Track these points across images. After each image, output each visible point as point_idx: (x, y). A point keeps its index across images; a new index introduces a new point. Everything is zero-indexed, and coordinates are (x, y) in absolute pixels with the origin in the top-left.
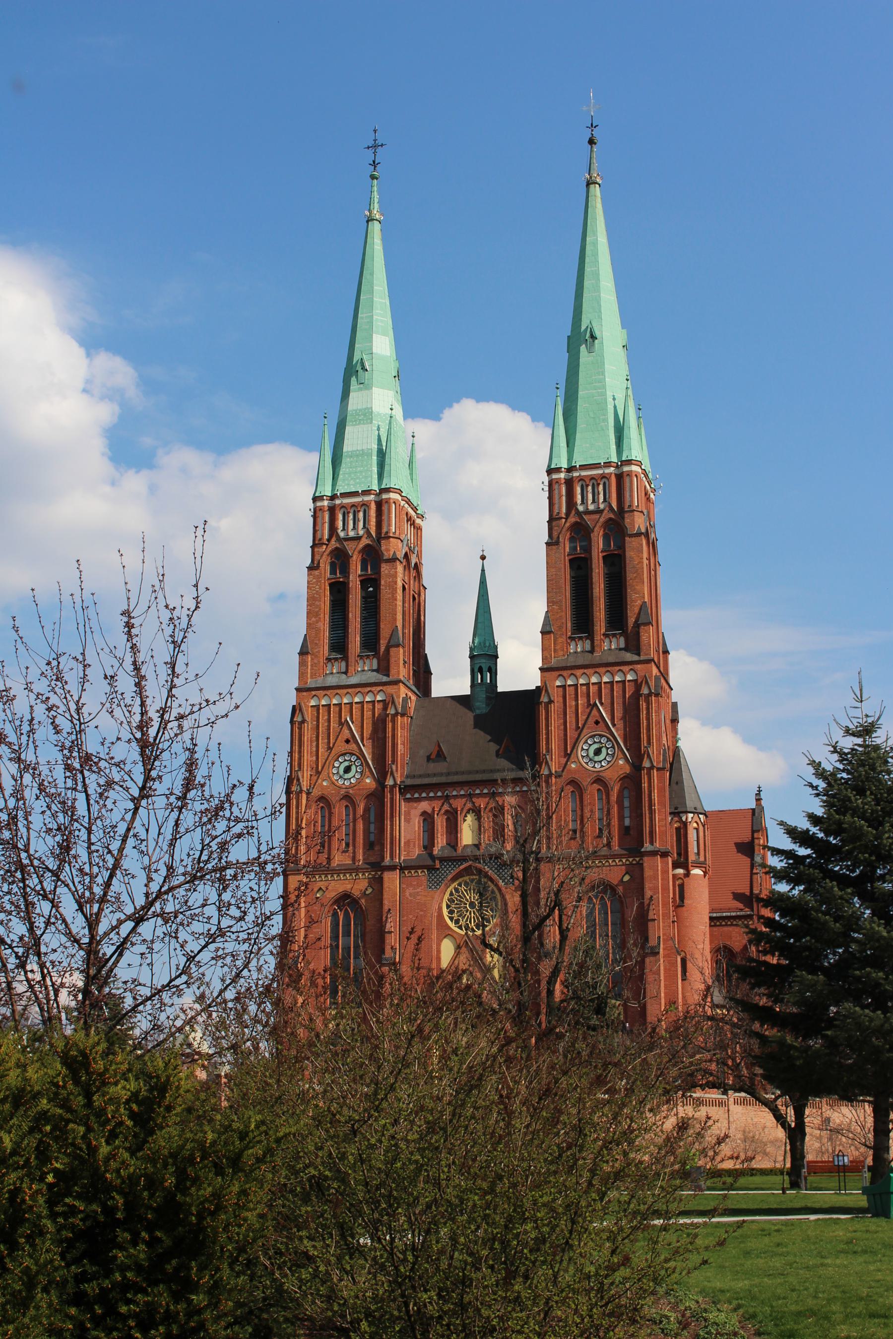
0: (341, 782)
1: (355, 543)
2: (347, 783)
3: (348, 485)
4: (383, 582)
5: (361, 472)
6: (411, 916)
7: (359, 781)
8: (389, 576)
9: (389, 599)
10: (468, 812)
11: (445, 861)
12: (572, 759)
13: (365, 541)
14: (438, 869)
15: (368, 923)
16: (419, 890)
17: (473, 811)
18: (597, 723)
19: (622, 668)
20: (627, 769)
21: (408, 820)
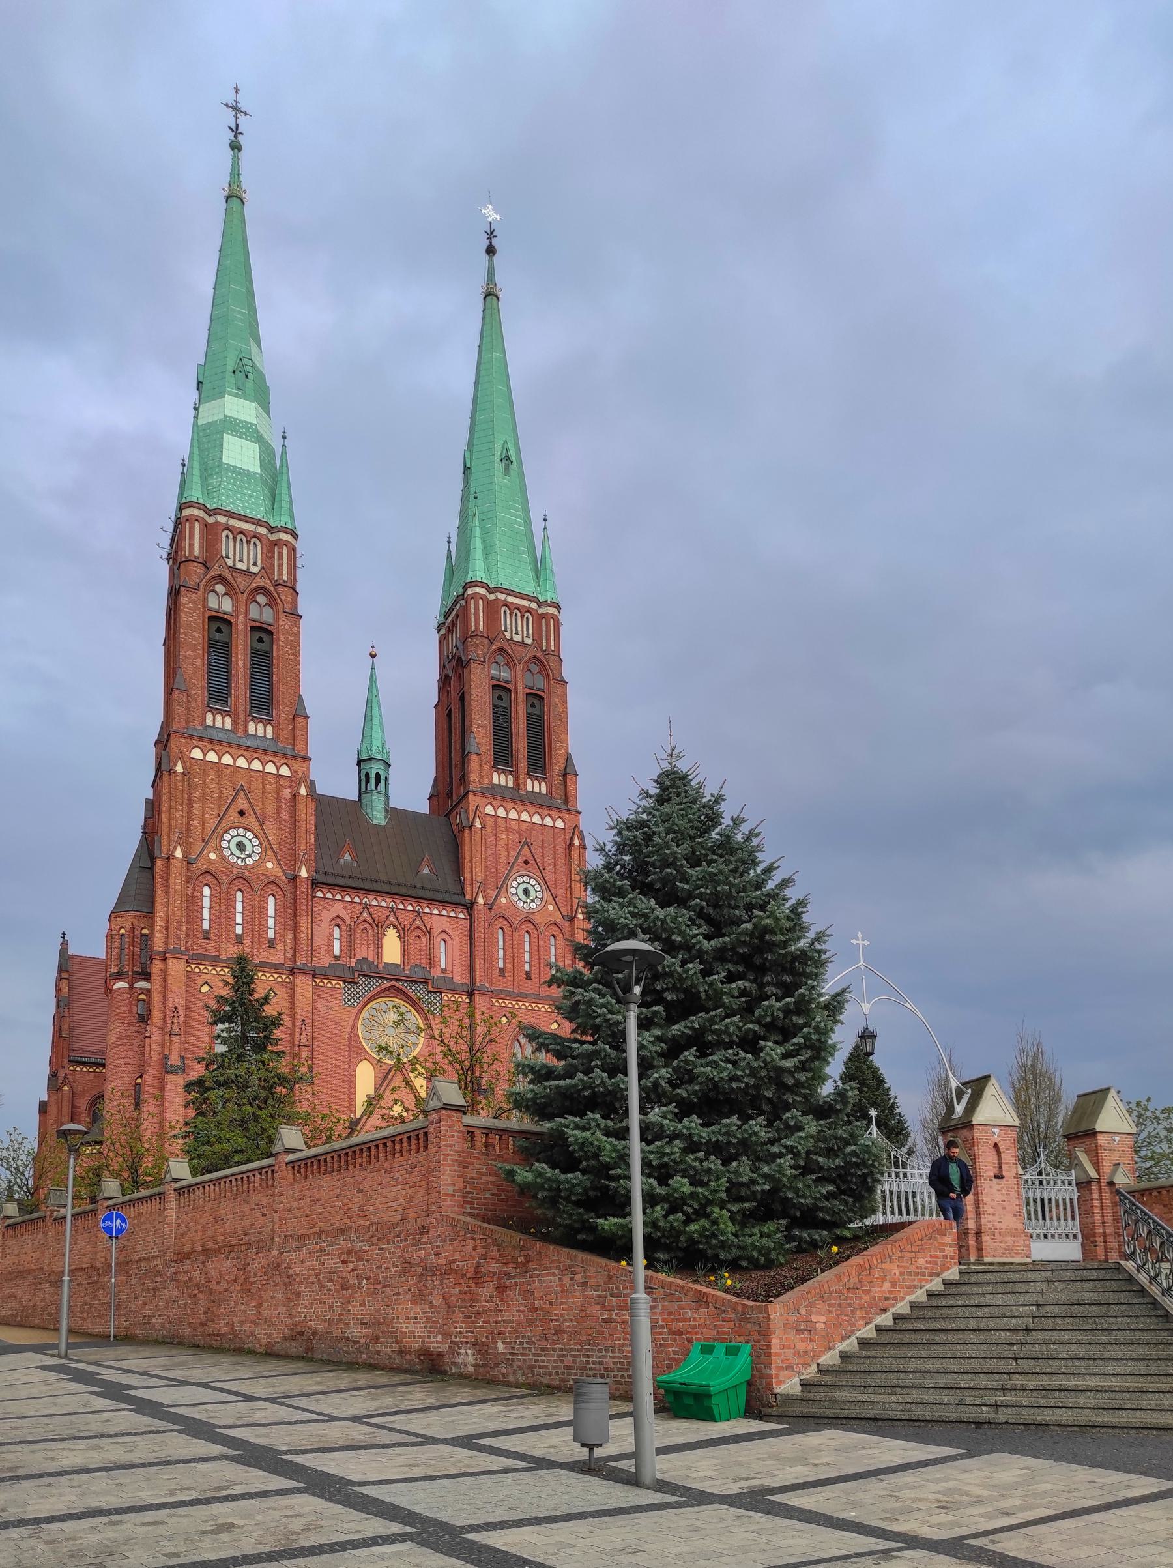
0: (233, 859)
1: (248, 579)
4: (282, 638)
10: (388, 927)
11: (364, 976)
13: (259, 582)
14: (356, 983)
16: (333, 1003)
17: (395, 927)
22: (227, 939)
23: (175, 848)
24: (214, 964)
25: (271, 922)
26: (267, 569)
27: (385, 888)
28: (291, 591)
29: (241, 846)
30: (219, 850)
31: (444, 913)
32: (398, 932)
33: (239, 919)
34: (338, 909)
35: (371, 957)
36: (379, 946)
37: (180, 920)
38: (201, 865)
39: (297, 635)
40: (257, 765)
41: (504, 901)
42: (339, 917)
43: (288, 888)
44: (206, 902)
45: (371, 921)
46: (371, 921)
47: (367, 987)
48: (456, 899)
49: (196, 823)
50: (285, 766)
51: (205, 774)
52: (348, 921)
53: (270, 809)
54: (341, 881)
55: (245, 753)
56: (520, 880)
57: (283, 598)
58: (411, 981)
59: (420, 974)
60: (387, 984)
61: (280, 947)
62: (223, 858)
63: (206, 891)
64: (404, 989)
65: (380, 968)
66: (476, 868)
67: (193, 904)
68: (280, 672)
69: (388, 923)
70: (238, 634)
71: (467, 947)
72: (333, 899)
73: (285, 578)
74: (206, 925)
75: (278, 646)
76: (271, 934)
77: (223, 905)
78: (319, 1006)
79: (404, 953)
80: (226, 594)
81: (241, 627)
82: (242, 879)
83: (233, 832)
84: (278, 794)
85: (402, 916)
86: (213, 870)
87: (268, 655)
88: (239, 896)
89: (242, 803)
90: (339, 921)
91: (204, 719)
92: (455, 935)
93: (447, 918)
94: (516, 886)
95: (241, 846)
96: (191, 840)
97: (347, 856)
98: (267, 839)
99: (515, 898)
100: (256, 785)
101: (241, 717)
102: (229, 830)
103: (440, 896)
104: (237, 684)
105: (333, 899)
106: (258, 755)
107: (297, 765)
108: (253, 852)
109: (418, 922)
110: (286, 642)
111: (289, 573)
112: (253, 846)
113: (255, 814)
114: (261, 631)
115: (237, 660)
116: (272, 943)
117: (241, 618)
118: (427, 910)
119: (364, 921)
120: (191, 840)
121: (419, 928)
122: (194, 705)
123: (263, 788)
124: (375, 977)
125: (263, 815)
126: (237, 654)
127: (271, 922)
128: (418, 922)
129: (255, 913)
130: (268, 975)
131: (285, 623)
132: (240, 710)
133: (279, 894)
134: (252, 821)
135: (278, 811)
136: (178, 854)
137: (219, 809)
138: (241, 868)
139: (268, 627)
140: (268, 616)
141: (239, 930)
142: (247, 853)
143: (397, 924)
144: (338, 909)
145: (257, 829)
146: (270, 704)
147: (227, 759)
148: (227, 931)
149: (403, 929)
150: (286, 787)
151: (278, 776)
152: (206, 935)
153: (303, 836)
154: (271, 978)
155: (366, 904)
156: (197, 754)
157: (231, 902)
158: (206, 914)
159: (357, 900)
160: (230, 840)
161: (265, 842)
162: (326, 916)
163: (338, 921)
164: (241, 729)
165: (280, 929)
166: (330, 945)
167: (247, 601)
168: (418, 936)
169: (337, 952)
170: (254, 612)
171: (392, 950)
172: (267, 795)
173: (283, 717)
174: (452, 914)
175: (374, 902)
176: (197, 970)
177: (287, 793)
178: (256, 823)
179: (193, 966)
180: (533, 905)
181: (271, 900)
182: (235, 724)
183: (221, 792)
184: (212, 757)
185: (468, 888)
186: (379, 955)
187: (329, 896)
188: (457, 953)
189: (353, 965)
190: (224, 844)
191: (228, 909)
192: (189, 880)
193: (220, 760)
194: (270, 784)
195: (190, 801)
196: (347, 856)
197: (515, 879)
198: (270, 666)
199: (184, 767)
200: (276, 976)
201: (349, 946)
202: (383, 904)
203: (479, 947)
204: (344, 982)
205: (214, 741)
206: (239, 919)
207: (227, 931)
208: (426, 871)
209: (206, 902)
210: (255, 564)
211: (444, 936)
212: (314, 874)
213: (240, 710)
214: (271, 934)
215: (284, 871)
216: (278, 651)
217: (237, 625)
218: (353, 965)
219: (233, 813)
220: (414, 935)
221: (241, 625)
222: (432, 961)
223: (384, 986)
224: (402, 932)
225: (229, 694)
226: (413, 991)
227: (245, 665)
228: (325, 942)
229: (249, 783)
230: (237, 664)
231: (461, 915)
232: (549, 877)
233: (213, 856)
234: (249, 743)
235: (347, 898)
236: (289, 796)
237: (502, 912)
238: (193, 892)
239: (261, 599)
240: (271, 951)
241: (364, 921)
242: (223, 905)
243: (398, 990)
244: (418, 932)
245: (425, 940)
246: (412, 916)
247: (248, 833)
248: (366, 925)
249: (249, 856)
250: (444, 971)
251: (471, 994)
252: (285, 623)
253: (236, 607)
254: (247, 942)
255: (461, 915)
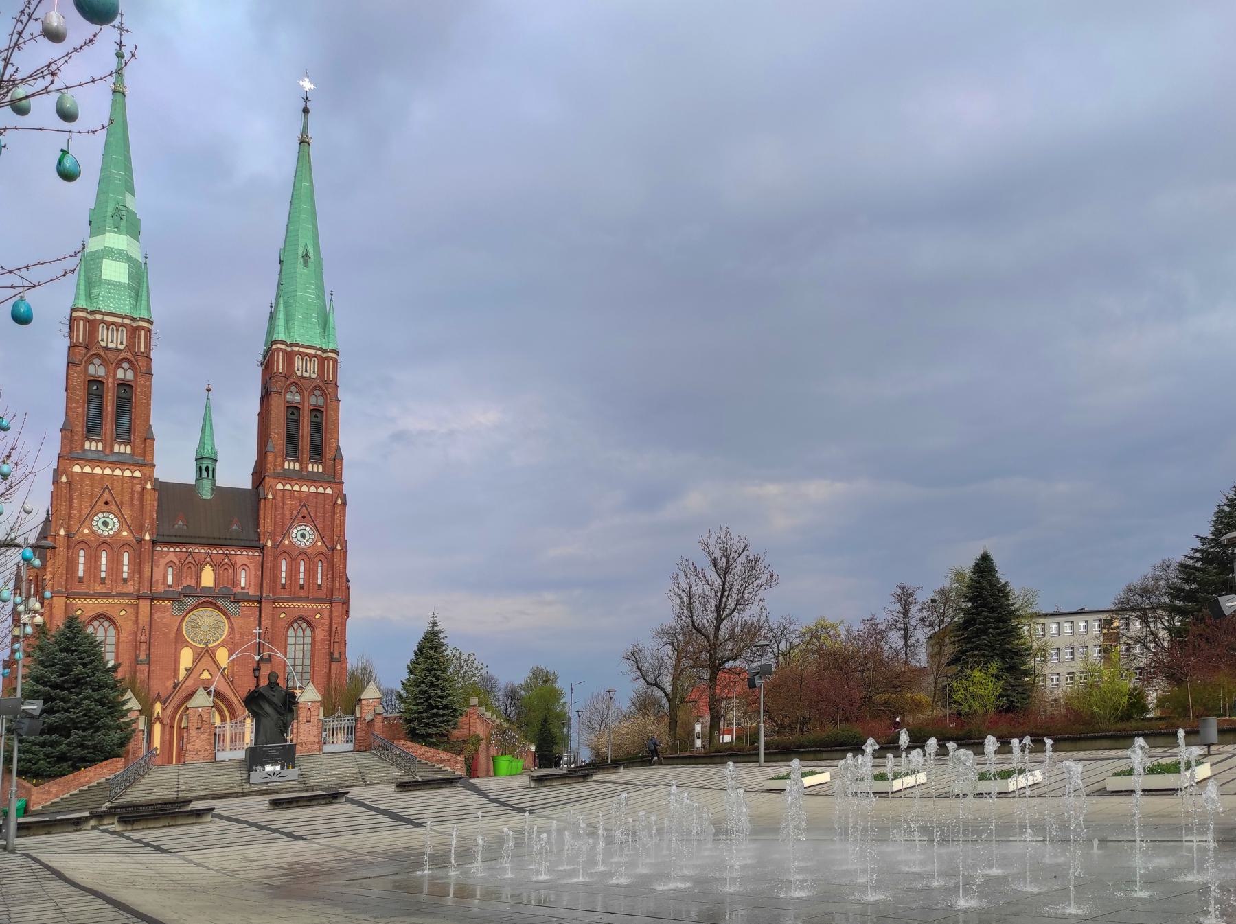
0: (100, 532)
2: (105, 534)
3: (108, 306)
4: (139, 390)
5: (120, 300)
6: (158, 632)
7: (117, 534)
8: (144, 386)
9: (145, 403)
10: (206, 564)
12: (285, 538)
13: (124, 355)
15: (121, 636)
17: (210, 564)
18: (304, 517)
19: (323, 485)
20: (324, 550)
21: (158, 567)
22: (95, 582)
23: (60, 529)
24: (85, 597)
25: (125, 568)
26: (131, 345)
27: (204, 541)
28: (146, 358)
29: (105, 524)
30: (90, 527)
31: (245, 553)
32: (212, 567)
33: (103, 568)
34: (171, 557)
35: (193, 584)
36: (198, 577)
37: (62, 573)
38: (78, 538)
39: (150, 386)
40: (118, 472)
41: (287, 542)
42: (172, 561)
43: (136, 547)
44: (81, 560)
45: (194, 562)
46: (194, 562)
47: (189, 602)
48: (253, 544)
49: (75, 512)
50: (138, 471)
51: (82, 480)
52: (178, 563)
53: (127, 498)
54: (174, 540)
55: (110, 465)
56: (299, 528)
57: (140, 364)
58: (217, 597)
59: (225, 591)
60: (203, 600)
61: (130, 583)
62: (93, 532)
63: (82, 553)
64: (213, 601)
65: (199, 590)
66: (267, 524)
67: (71, 563)
68: (137, 411)
69: (205, 562)
70: (108, 390)
71: (260, 573)
72: (168, 551)
73: (142, 350)
74: (81, 574)
75: (136, 394)
76: (125, 575)
77: (93, 560)
78: (156, 617)
79: (216, 580)
80: (101, 364)
81: (110, 385)
82: (105, 543)
83: (100, 515)
84: (132, 489)
85: (215, 557)
86: (85, 539)
87: (129, 400)
88: (104, 554)
89: (107, 496)
90: (171, 564)
91: (83, 445)
92: (251, 566)
93: (246, 556)
94: (296, 533)
95: (105, 524)
96: (72, 522)
97: (180, 523)
98: (124, 518)
99: (295, 540)
100: (117, 485)
101: (109, 442)
102: (98, 514)
103: (242, 543)
104: (106, 421)
105: (168, 551)
106: (118, 466)
107: (147, 471)
108: (114, 526)
109: (226, 560)
110: (141, 392)
111: (146, 347)
112: (114, 523)
113: (116, 503)
114: (124, 386)
115: (107, 406)
116: (125, 581)
117: (111, 380)
118: (233, 552)
119: (189, 562)
120: (72, 522)
121: (226, 564)
122: (76, 438)
123: (122, 485)
124: (195, 596)
125: (122, 503)
126: (107, 402)
127: (125, 568)
128: (226, 560)
129: (115, 563)
130: (121, 601)
131: (141, 380)
132: (108, 438)
133: (131, 551)
134: (114, 508)
135: (132, 499)
136: (62, 532)
137: (91, 502)
138: (105, 537)
139: (130, 383)
140: (130, 375)
141: (103, 575)
142: (110, 527)
143: (212, 563)
144: (171, 557)
145: (117, 511)
146: (130, 431)
147: (98, 470)
148: (95, 576)
149: (216, 565)
150: (138, 484)
151: (133, 478)
152: (81, 580)
153: (148, 514)
154: (124, 603)
155: (190, 552)
156: (77, 469)
157: (97, 559)
158: (81, 567)
159: (184, 550)
160: (97, 521)
161: (122, 519)
162: (163, 562)
163: (171, 564)
164: (108, 450)
165: (132, 572)
166: (165, 578)
167: (115, 368)
168: (226, 569)
169: (170, 581)
170: (120, 374)
171: (208, 578)
172: (125, 490)
173: (138, 440)
174: (250, 553)
175: (197, 551)
176: (74, 602)
177: (138, 488)
178: (116, 509)
179: (71, 600)
180: (308, 543)
181: (126, 556)
182: (104, 447)
183: (92, 492)
184: (87, 470)
185: (262, 536)
186: (198, 582)
187: (165, 549)
188: (253, 577)
189: (180, 590)
190: (94, 523)
191: (96, 562)
192: (68, 547)
193: (92, 471)
194: (127, 483)
195: (71, 499)
196: (180, 523)
197: (295, 528)
198: (130, 407)
199: (67, 479)
200: (127, 601)
201: (178, 578)
202: (203, 551)
203: (267, 573)
204: (173, 601)
205: (88, 460)
206: (103, 568)
207: (95, 576)
208: (235, 527)
209: (81, 560)
210: (122, 343)
211: (244, 567)
212: (155, 536)
213: (108, 438)
214: (125, 575)
215: (135, 537)
216: (135, 398)
217: (108, 384)
218: (180, 590)
219: (101, 503)
220: (223, 568)
221: (110, 383)
222: (235, 582)
223: (200, 602)
224: (215, 568)
225: (101, 428)
226: (219, 602)
227: (113, 409)
228: (161, 577)
229: (112, 484)
230: (107, 409)
231: (257, 554)
232: (320, 526)
233: (86, 531)
234: (113, 458)
235: (178, 550)
236: (140, 490)
237: (285, 549)
238: (72, 555)
239: (126, 365)
240: (124, 586)
241: (189, 562)
242: (93, 560)
243: (211, 603)
244: (226, 566)
245: (230, 571)
246: (222, 557)
247: (111, 515)
248: (191, 566)
249: (111, 529)
250: (243, 588)
251: (260, 602)
252: (141, 380)
253: (108, 372)
254: (108, 582)
255: (257, 554)
